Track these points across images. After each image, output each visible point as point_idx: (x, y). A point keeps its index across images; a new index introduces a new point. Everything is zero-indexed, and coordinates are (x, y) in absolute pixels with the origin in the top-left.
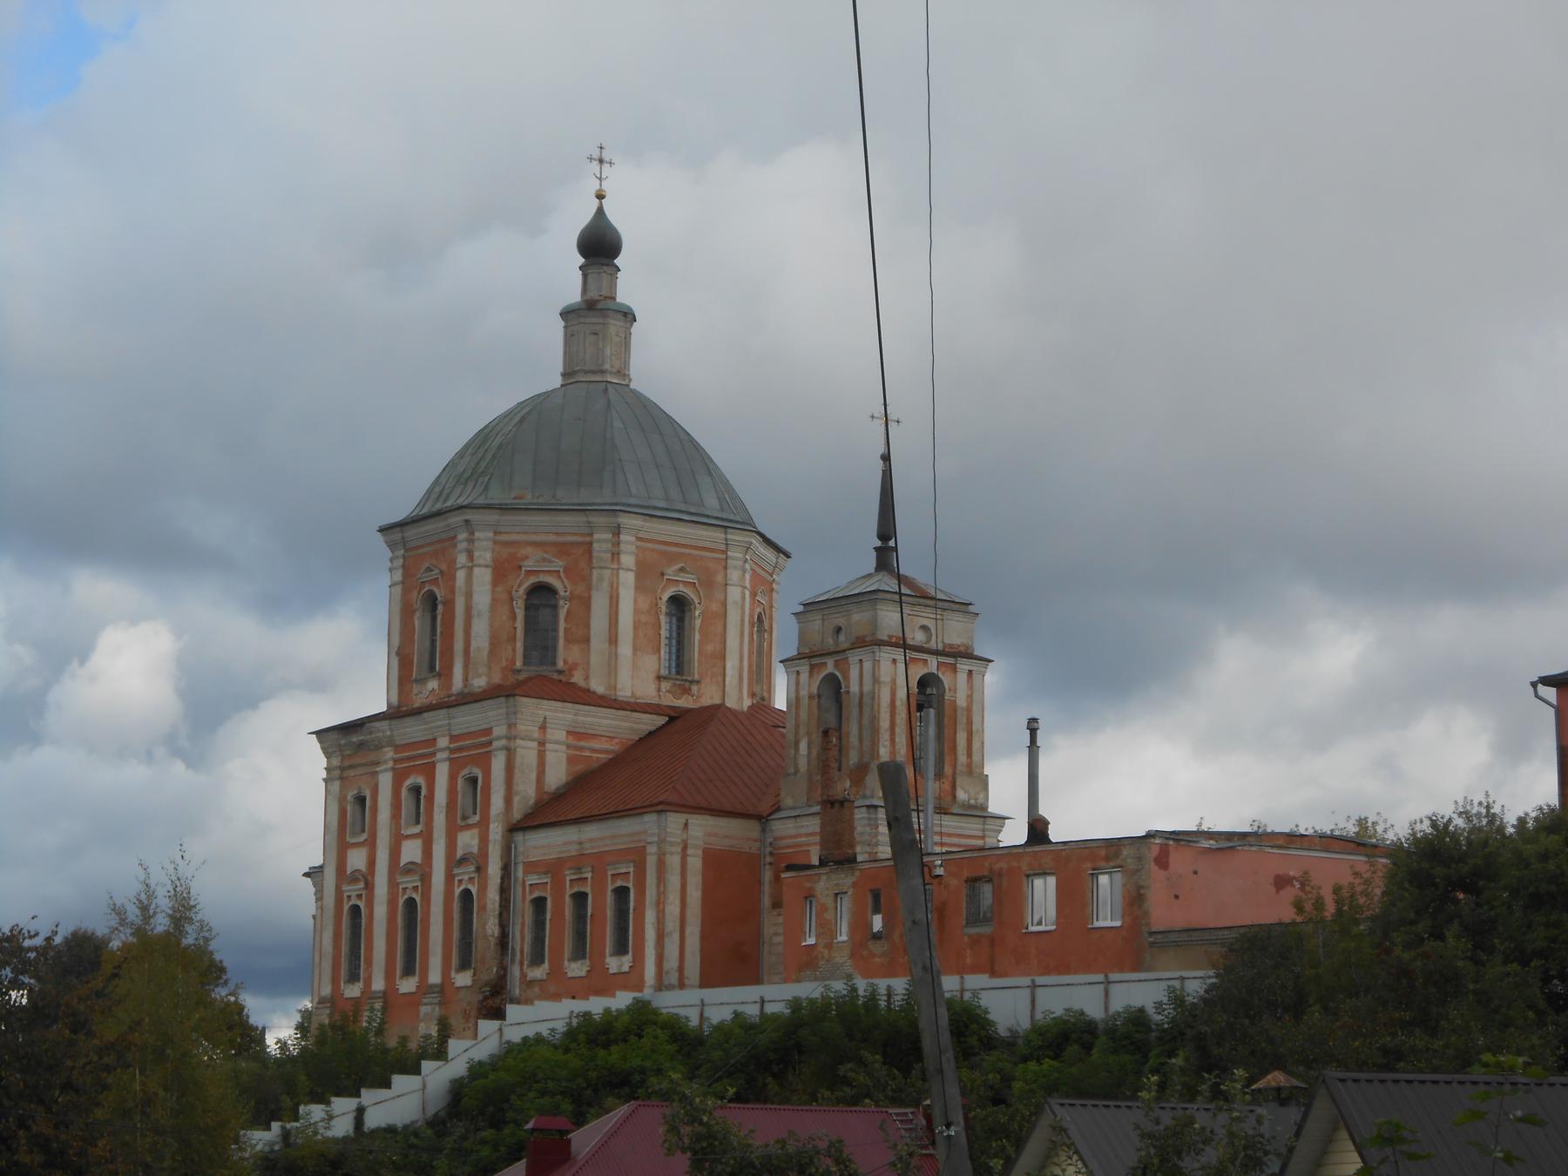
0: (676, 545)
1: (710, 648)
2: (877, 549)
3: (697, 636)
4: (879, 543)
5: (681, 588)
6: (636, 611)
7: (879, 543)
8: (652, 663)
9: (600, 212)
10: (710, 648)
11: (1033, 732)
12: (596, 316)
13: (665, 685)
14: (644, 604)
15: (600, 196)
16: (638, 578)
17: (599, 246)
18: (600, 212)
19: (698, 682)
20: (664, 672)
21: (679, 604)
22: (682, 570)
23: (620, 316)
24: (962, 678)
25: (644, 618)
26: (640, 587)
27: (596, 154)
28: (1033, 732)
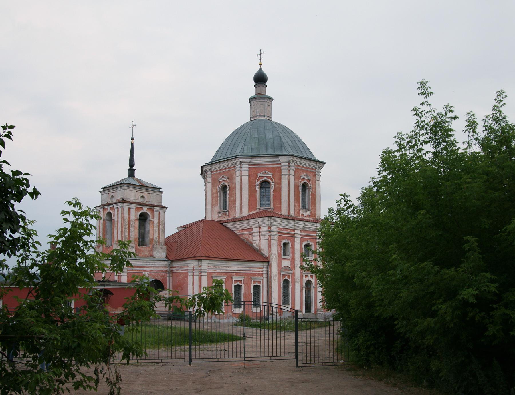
0: (223, 170)
3: (228, 196)
4: (130, 168)
5: (223, 183)
6: (212, 194)
7: (130, 168)
8: (217, 208)
9: (260, 69)
12: (260, 99)
13: (220, 214)
14: (214, 191)
15: (260, 65)
17: (260, 79)
18: (260, 69)
19: (228, 211)
21: (224, 188)
22: (223, 177)
23: (254, 99)
25: (214, 195)
27: (262, 52)
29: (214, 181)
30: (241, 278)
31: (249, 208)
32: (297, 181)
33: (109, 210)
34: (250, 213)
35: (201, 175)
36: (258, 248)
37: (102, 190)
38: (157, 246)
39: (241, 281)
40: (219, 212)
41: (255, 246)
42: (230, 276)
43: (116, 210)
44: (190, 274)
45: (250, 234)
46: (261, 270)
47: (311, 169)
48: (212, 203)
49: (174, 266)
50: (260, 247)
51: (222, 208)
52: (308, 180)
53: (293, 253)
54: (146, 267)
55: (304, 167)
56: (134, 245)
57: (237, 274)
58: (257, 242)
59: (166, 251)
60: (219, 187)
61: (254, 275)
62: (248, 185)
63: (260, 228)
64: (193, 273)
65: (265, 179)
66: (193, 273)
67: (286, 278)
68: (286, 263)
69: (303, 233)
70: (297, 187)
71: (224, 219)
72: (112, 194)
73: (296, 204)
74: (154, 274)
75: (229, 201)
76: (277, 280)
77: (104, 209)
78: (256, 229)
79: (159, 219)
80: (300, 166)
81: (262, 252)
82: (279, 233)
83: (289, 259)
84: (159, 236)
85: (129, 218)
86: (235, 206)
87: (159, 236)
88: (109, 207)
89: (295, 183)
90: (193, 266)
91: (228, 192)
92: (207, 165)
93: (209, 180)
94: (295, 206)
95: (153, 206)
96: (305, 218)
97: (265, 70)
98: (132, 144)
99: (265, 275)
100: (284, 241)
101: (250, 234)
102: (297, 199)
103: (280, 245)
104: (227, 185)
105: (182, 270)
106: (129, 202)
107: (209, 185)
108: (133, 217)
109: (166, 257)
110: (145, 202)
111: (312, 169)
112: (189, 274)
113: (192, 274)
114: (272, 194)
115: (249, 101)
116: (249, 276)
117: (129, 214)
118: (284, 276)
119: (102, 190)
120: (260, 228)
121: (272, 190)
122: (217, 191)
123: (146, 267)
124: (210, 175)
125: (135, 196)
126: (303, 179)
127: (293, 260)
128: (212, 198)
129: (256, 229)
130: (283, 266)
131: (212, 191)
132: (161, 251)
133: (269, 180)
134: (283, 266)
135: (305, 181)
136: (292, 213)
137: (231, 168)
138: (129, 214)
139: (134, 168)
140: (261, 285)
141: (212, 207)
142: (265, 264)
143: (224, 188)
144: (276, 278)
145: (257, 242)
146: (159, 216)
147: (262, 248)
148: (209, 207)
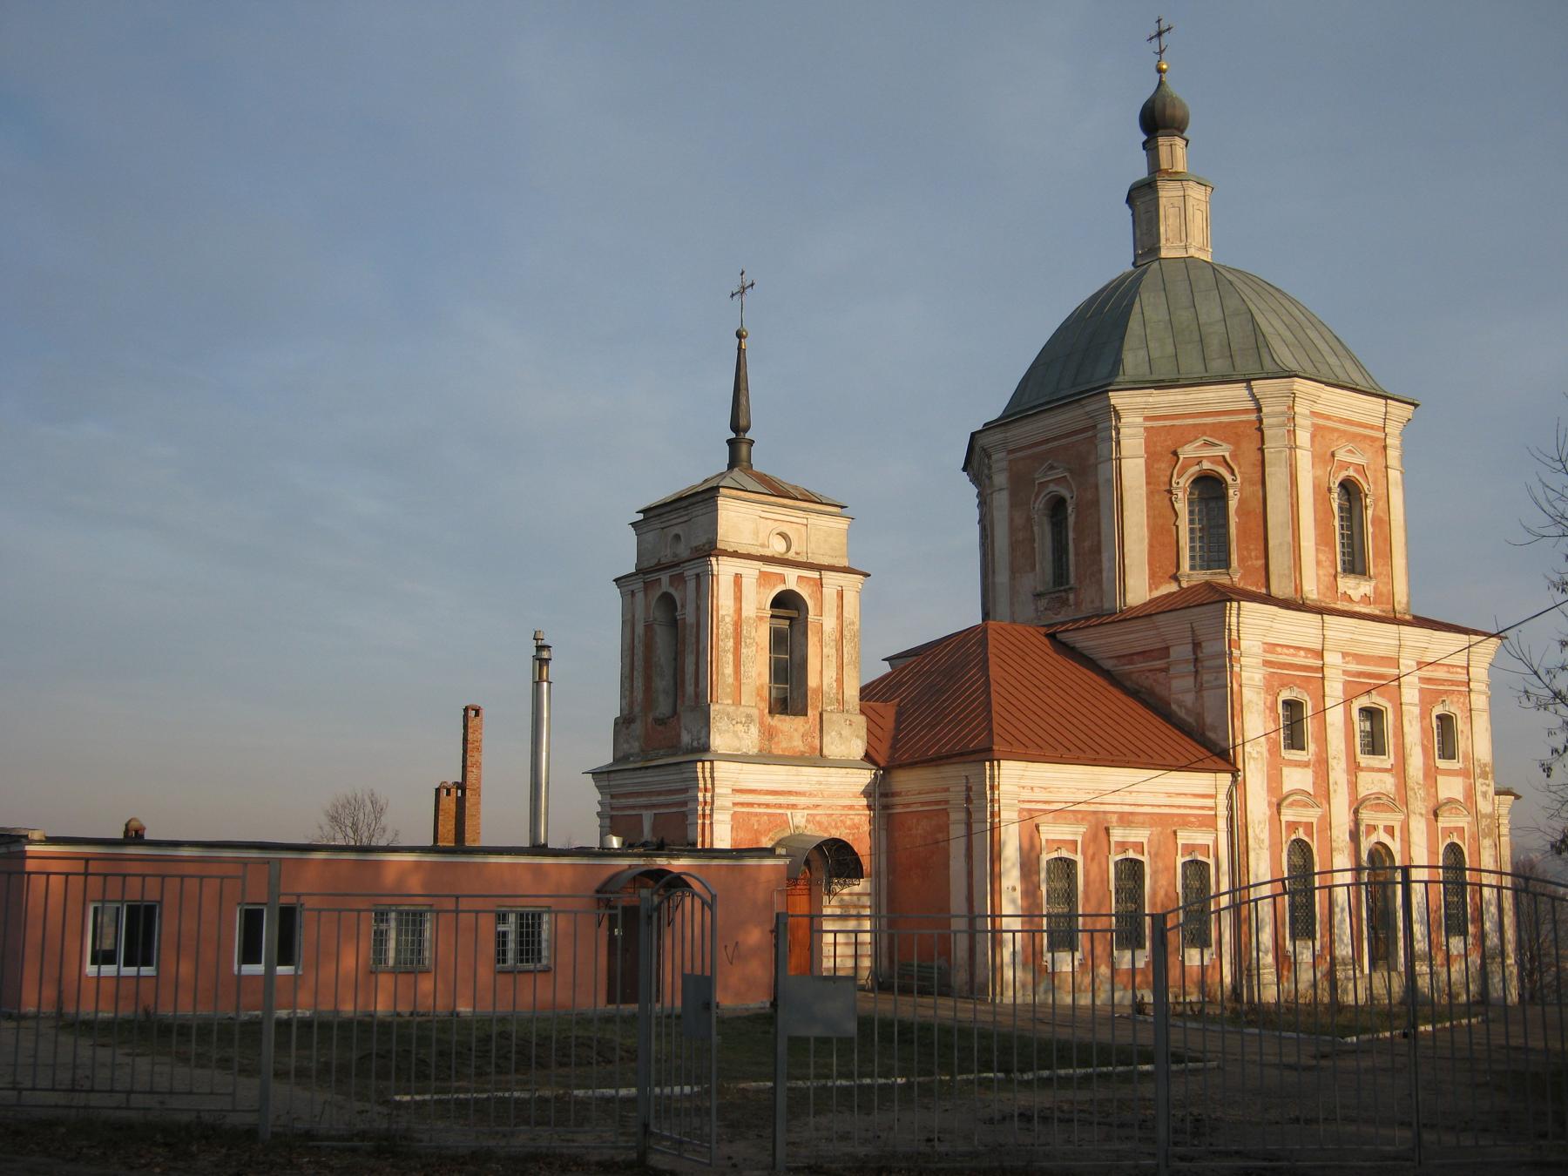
0: (1047, 441)
1: (1087, 544)
2: (730, 442)
3: (1071, 535)
5: (1052, 487)
6: (1013, 530)
9: (1161, 83)
10: (1087, 544)
11: (542, 662)
13: (1043, 603)
16: (1013, 495)
20: (1040, 589)
21: (1057, 507)
22: (1052, 468)
24: (692, 585)
26: (1014, 504)
27: (1164, 26)
28: (542, 662)
29: (1020, 485)
30: (1140, 835)
31: (1152, 576)
32: (1319, 472)
33: (665, 585)
34: (1156, 594)
35: (964, 469)
36: (1190, 720)
37: (641, 516)
38: (835, 717)
39: (1139, 847)
40: (1038, 596)
41: (1182, 714)
42: (1100, 830)
43: (692, 585)
44: (957, 816)
45: (1162, 670)
46: (1210, 803)
47: (1365, 426)
48: (1012, 564)
49: (897, 788)
50: (1200, 716)
51: (1049, 577)
52: (1361, 469)
53: (1323, 741)
54: (797, 793)
55: (1341, 421)
56: (755, 712)
57: (1126, 819)
58: (1189, 699)
59: (864, 733)
60: (1040, 504)
61: (1184, 821)
62: (1144, 491)
63: (1197, 645)
64: (969, 813)
65: (1206, 465)
66: (969, 813)
67: (1301, 834)
68: (1297, 779)
69: (1354, 667)
70: (1322, 493)
71: (1060, 618)
72: (677, 530)
73: (1322, 557)
74: (824, 820)
75: (1077, 554)
76: (1267, 843)
77: (647, 586)
78: (1181, 651)
79: (840, 616)
80: (1328, 418)
81: (1211, 735)
82: (1267, 663)
83: (1306, 765)
84: (840, 681)
85: (739, 610)
86: (1100, 571)
87: (840, 681)
88: (665, 578)
89: (1315, 478)
90: (969, 789)
91: (1071, 520)
92: (989, 427)
93: (1000, 479)
94: (1318, 563)
95: (819, 568)
96: (1357, 608)
97: (1175, 88)
98: (739, 348)
99: (1222, 824)
100: (1286, 694)
101: (1162, 670)
102: (1323, 539)
103: (1273, 708)
104: (1067, 495)
105: (923, 804)
106: (735, 554)
107: (1001, 500)
108: (749, 610)
109: (868, 757)
110: (791, 555)
111: (1372, 427)
112: (954, 816)
113: (962, 816)
114: (1233, 520)
115: (1128, 201)
116: (1169, 824)
117: (738, 598)
118: (1293, 826)
119: (641, 516)
120: (1197, 645)
121: (1233, 504)
122: (1029, 519)
123: (797, 793)
124: (1004, 464)
125: (756, 533)
126: (1347, 465)
127: (1321, 766)
128: (1013, 547)
129: (1181, 651)
130: (1286, 789)
131: (1012, 520)
132: (846, 732)
133: (1223, 471)
134: (1286, 789)
135: (1351, 472)
136: (1311, 590)
137: (1075, 433)
138: (738, 598)
139: (748, 436)
140: (1211, 862)
141: (1013, 577)
142: (1225, 779)
143: (1057, 507)
144: (1265, 836)
145: (1189, 699)
146: (841, 607)
147: (1208, 720)
148: (1002, 578)
